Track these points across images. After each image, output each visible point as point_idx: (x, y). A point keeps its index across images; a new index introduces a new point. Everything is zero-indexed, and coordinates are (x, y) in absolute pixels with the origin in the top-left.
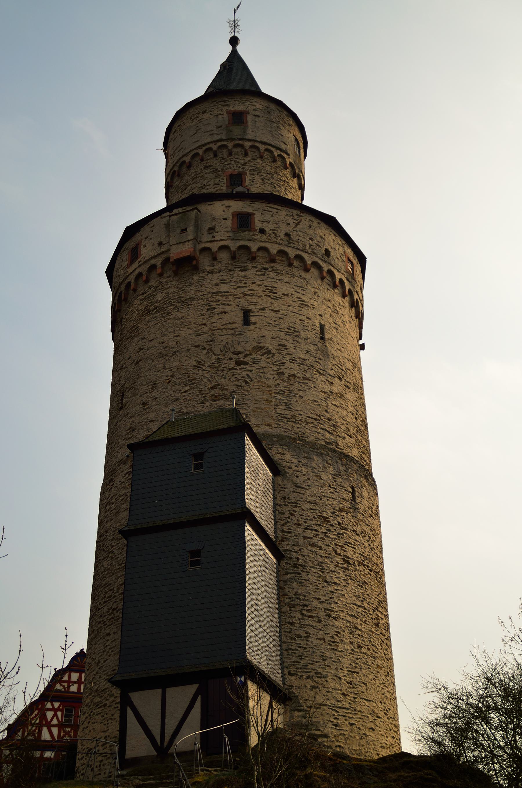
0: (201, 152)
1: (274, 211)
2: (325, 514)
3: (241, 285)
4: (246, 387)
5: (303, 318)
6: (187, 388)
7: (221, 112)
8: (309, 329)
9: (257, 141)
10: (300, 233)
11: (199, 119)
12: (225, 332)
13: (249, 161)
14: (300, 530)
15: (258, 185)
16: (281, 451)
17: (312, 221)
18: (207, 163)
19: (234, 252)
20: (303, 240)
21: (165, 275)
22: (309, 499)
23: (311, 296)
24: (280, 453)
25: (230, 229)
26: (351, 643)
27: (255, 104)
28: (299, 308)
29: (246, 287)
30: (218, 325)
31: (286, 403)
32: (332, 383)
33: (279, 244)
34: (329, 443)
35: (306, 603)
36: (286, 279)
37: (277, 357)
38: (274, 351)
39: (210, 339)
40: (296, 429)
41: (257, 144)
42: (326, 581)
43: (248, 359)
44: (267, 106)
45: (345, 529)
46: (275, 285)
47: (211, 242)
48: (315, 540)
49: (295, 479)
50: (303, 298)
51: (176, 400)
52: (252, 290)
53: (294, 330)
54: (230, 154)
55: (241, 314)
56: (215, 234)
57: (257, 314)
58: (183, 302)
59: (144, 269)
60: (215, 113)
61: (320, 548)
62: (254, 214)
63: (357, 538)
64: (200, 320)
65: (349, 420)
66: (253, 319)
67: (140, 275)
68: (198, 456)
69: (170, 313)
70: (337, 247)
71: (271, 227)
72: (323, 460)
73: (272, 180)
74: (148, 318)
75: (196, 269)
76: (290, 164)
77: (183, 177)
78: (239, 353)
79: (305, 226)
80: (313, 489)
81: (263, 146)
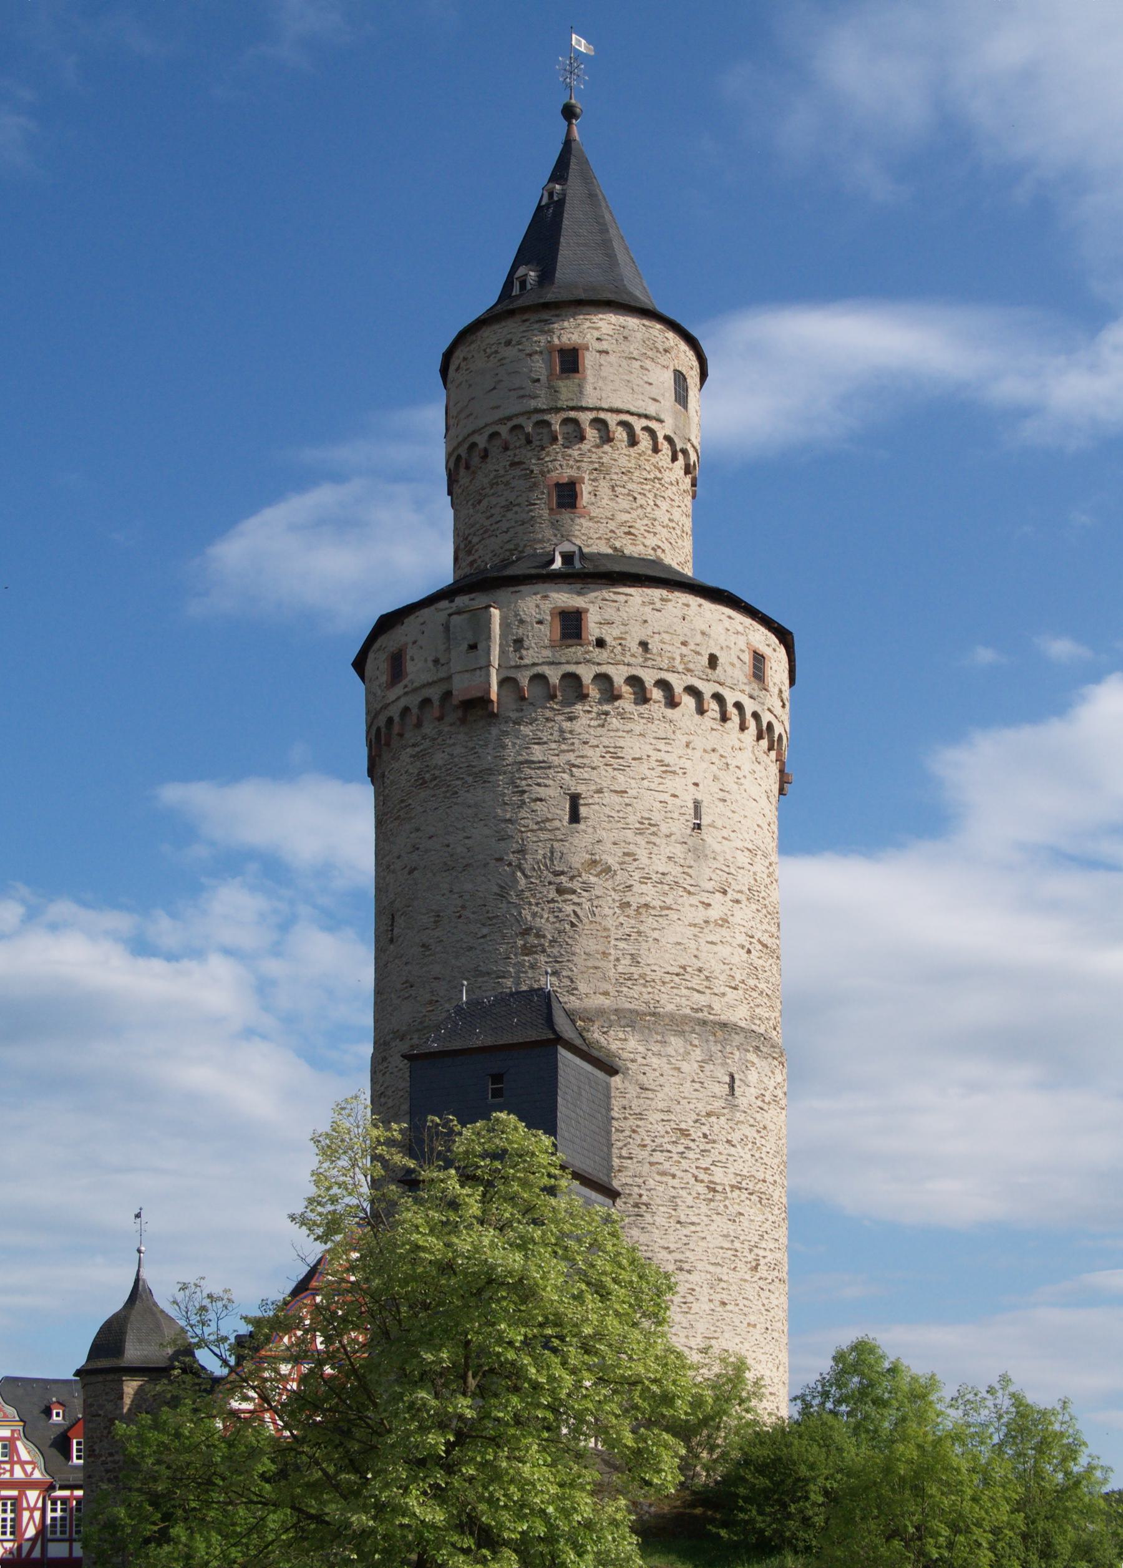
0: (504, 430)
1: (622, 598)
2: (683, 1126)
3: (564, 747)
5: (666, 797)
6: (485, 931)
8: (676, 815)
9: (603, 409)
10: (664, 636)
11: (499, 356)
13: (589, 451)
14: (645, 1154)
15: (604, 502)
16: (621, 1035)
17: (688, 605)
18: (515, 455)
20: (669, 648)
22: (661, 1105)
23: (680, 752)
24: (620, 1040)
26: (711, 1301)
27: (601, 324)
28: (660, 780)
29: (573, 751)
31: (632, 955)
33: (629, 665)
36: (638, 729)
37: (621, 877)
40: (646, 996)
41: (602, 415)
42: (679, 1222)
44: (624, 324)
45: (714, 1142)
46: (621, 743)
48: (666, 1165)
49: (641, 1077)
50: (668, 759)
51: (471, 948)
52: (582, 757)
53: (650, 824)
56: (524, 652)
57: (591, 801)
59: (413, 701)
61: (674, 1176)
62: (587, 611)
63: (732, 1150)
65: (735, 960)
66: (583, 811)
67: (406, 710)
69: (456, 793)
71: (616, 632)
72: (686, 1041)
73: (630, 486)
76: (668, 438)
77: (474, 473)
78: (562, 873)
79: (675, 620)
80: (666, 1089)
81: (614, 416)
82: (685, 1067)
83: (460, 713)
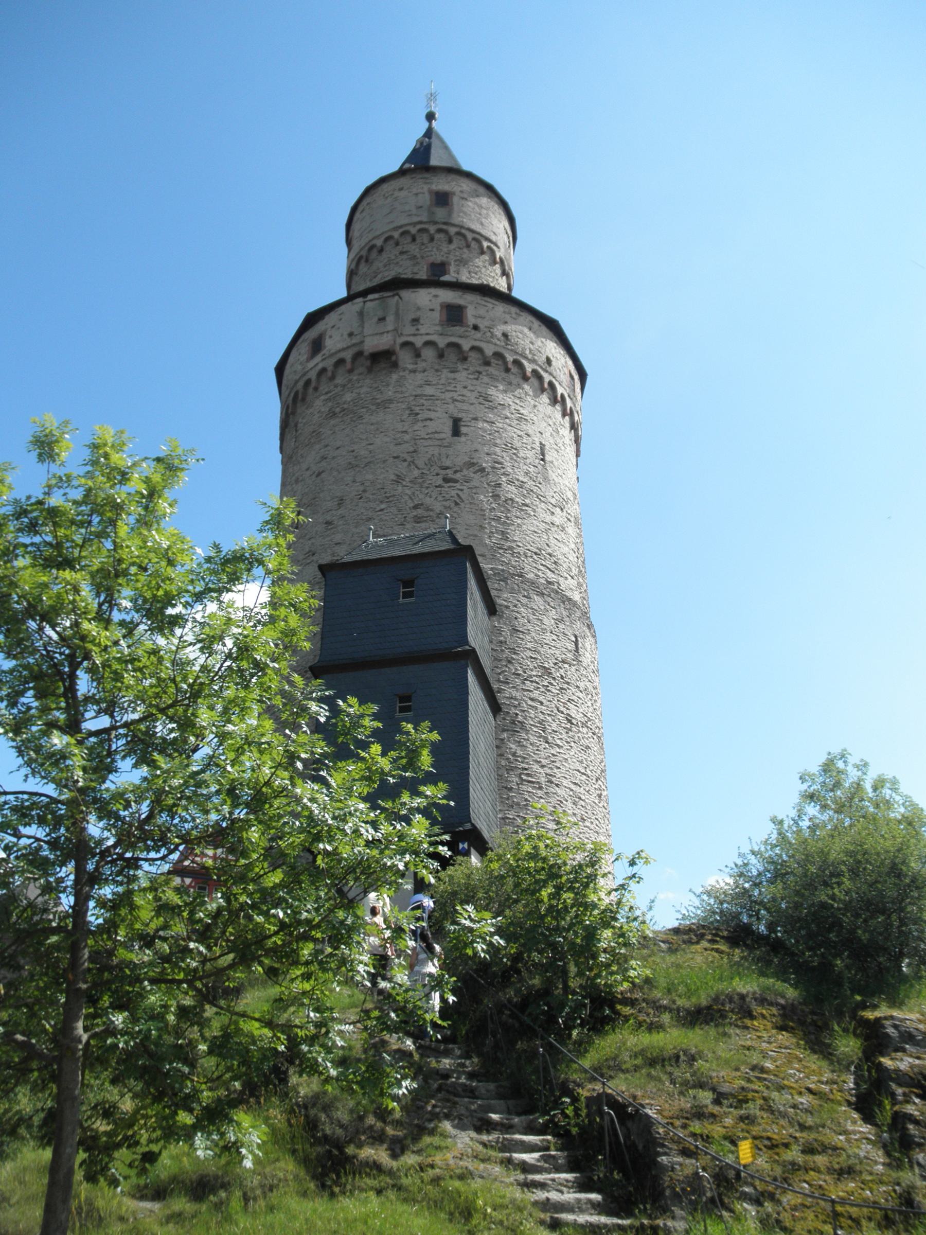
1: (490, 306)
4: (456, 509)
7: (419, 191)
12: (430, 442)
19: (443, 350)
21: (356, 372)
22: (529, 645)
25: (437, 322)
30: (423, 434)
32: (553, 513)
34: (550, 583)
35: (526, 766)
38: (488, 469)
39: (411, 449)
41: (463, 231)
43: (458, 476)
45: (568, 683)
47: (414, 335)
48: (535, 694)
50: (522, 411)
54: (432, 239)
55: (450, 423)
58: (378, 404)
59: (329, 363)
60: (415, 191)
61: (542, 703)
62: (466, 307)
63: (581, 695)
64: (400, 427)
66: (464, 430)
67: (323, 370)
68: (408, 583)
70: (559, 356)
71: (487, 323)
74: (332, 422)
75: (395, 365)
76: (501, 259)
78: (447, 468)
82: (546, 621)
83: (368, 363)
